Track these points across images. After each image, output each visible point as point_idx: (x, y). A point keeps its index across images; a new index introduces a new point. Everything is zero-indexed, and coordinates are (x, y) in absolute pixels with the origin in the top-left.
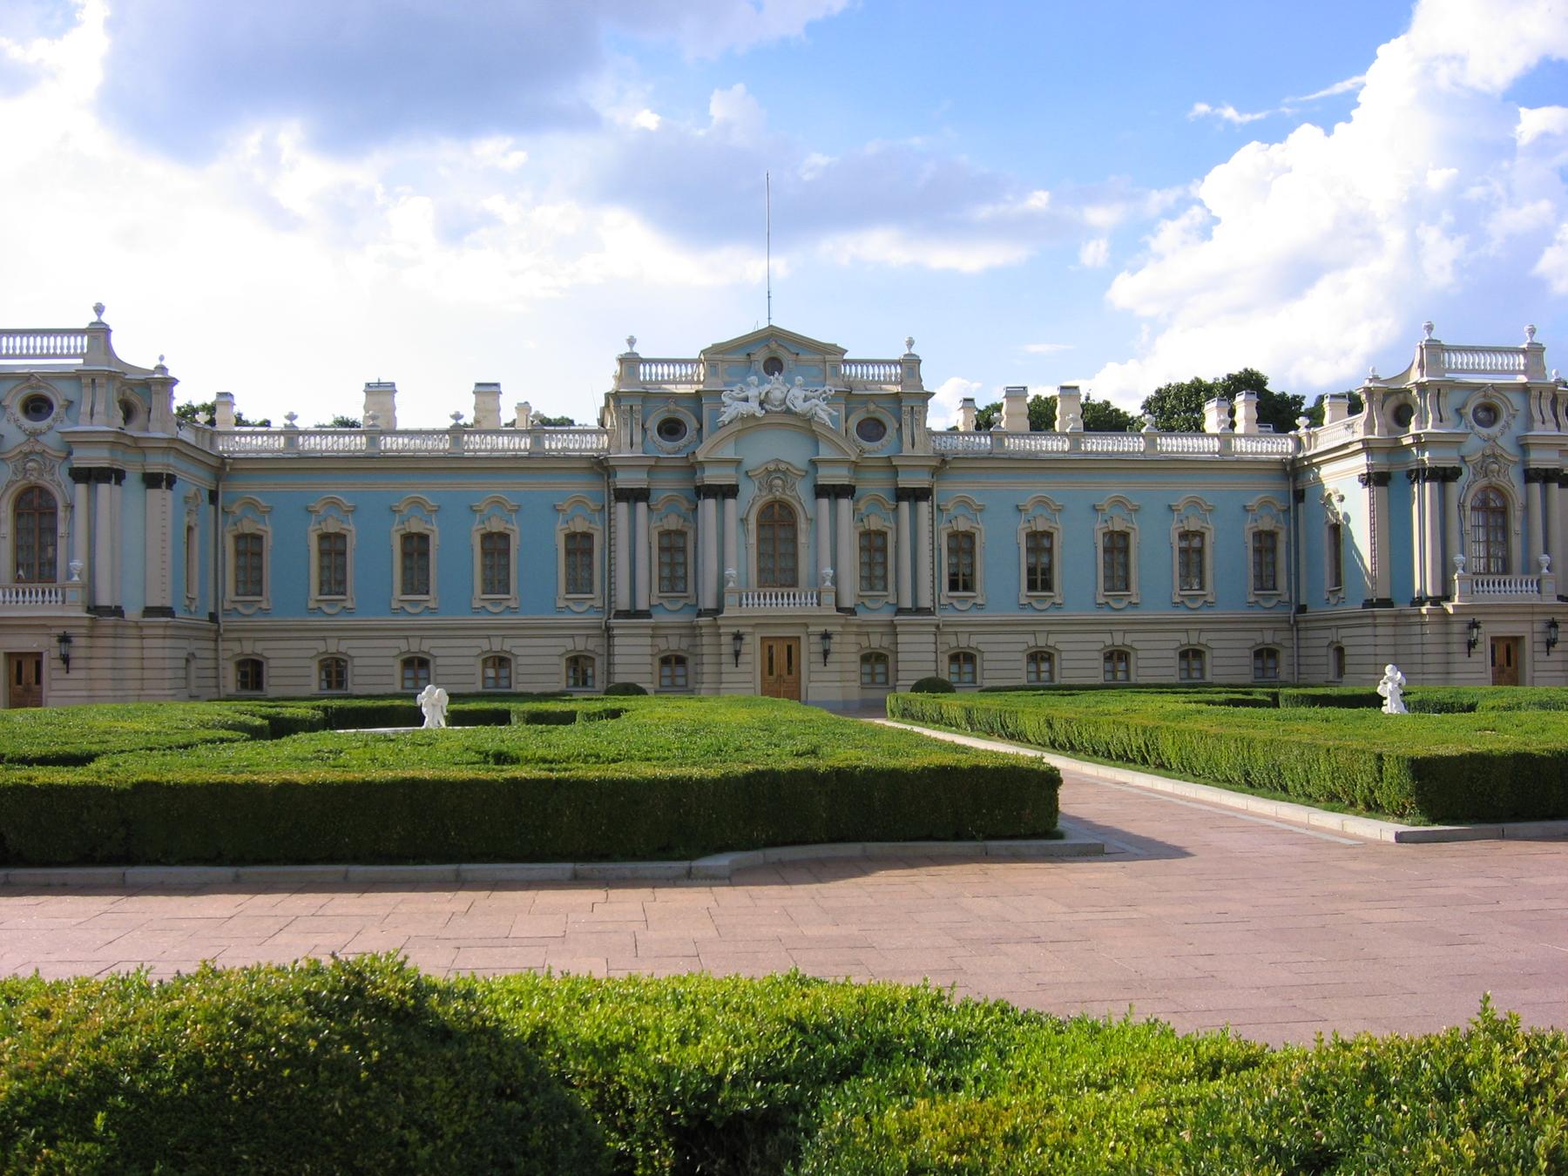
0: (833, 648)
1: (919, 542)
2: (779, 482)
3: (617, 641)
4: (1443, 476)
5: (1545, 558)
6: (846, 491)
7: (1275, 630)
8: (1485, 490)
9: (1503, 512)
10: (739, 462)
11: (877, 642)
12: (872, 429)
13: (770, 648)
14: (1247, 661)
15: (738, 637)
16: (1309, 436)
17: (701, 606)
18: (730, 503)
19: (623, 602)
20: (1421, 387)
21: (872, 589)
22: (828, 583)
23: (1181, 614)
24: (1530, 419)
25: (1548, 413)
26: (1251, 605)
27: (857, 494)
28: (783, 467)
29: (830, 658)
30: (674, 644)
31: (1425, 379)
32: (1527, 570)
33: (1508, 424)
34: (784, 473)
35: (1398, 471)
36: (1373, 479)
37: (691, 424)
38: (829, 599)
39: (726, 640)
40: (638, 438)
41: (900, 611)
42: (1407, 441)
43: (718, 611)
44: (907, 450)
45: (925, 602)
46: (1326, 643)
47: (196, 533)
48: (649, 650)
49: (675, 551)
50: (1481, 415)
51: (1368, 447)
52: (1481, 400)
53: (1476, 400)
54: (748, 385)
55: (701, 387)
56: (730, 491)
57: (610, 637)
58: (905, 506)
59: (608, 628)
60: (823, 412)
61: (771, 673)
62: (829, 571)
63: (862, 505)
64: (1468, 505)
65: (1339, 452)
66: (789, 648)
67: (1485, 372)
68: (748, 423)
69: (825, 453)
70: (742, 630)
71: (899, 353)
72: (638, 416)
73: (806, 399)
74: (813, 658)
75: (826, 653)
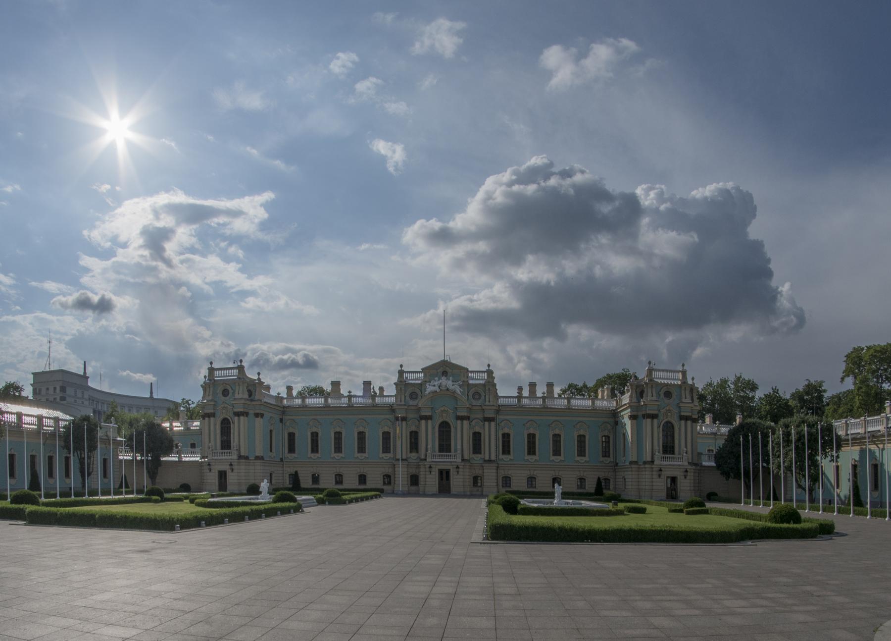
1: (491, 437)
4: (653, 417)
6: (468, 418)
11: (478, 472)
30: (413, 471)
35: (640, 414)
37: (420, 394)
44: (487, 403)
45: (493, 457)
47: (274, 433)
58: (487, 423)
63: (473, 423)
71: (485, 368)
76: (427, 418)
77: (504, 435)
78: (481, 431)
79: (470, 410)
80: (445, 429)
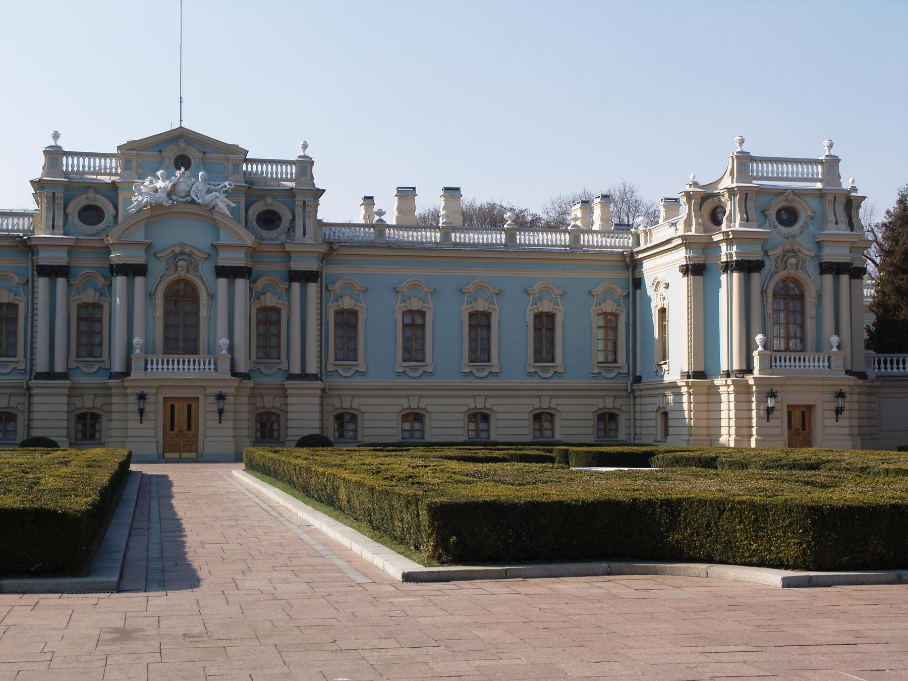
0: (227, 408)
2: (182, 263)
3: (35, 399)
5: (834, 339)
7: (615, 397)
8: (785, 280)
9: (801, 298)
10: (149, 245)
11: (270, 402)
12: (269, 220)
13: (173, 407)
14: (591, 423)
15: (142, 397)
16: (646, 233)
17: (112, 371)
18: (139, 281)
19: (41, 365)
20: (731, 192)
21: (267, 357)
22: (224, 352)
23: (535, 382)
24: (824, 218)
25: (842, 216)
26: (596, 376)
27: (254, 275)
28: (187, 250)
29: (226, 416)
30: (88, 403)
31: (735, 185)
32: (818, 349)
33: (806, 226)
34: (189, 255)
36: (693, 270)
37: (109, 210)
38: (225, 365)
39: (133, 399)
40: (60, 222)
41: (291, 377)
42: (717, 238)
43: (127, 373)
45: (312, 368)
46: (655, 408)
48: (65, 408)
49: (90, 322)
50: (784, 216)
51: (687, 242)
52: (784, 204)
53: (778, 203)
54: (158, 178)
55: (114, 178)
56: (139, 270)
57: (31, 396)
58: (296, 286)
59: (29, 388)
60: (223, 204)
61: (172, 428)
62: (224, 341)
63: (259, 285)
64: (770, 293)
65: (664, 247)
66: (189, 407)
67: (787, 179)
68: (156, 213)
69: (225, 238)
70: (146, 391)
72: (60, 202)
73: (209, 191)
74: (210, 416)
75: (221, 412)
76: (132, 271)
77: (339, 313)
78: (282, 304)
79: (252, 252)
80: (181, 301)
